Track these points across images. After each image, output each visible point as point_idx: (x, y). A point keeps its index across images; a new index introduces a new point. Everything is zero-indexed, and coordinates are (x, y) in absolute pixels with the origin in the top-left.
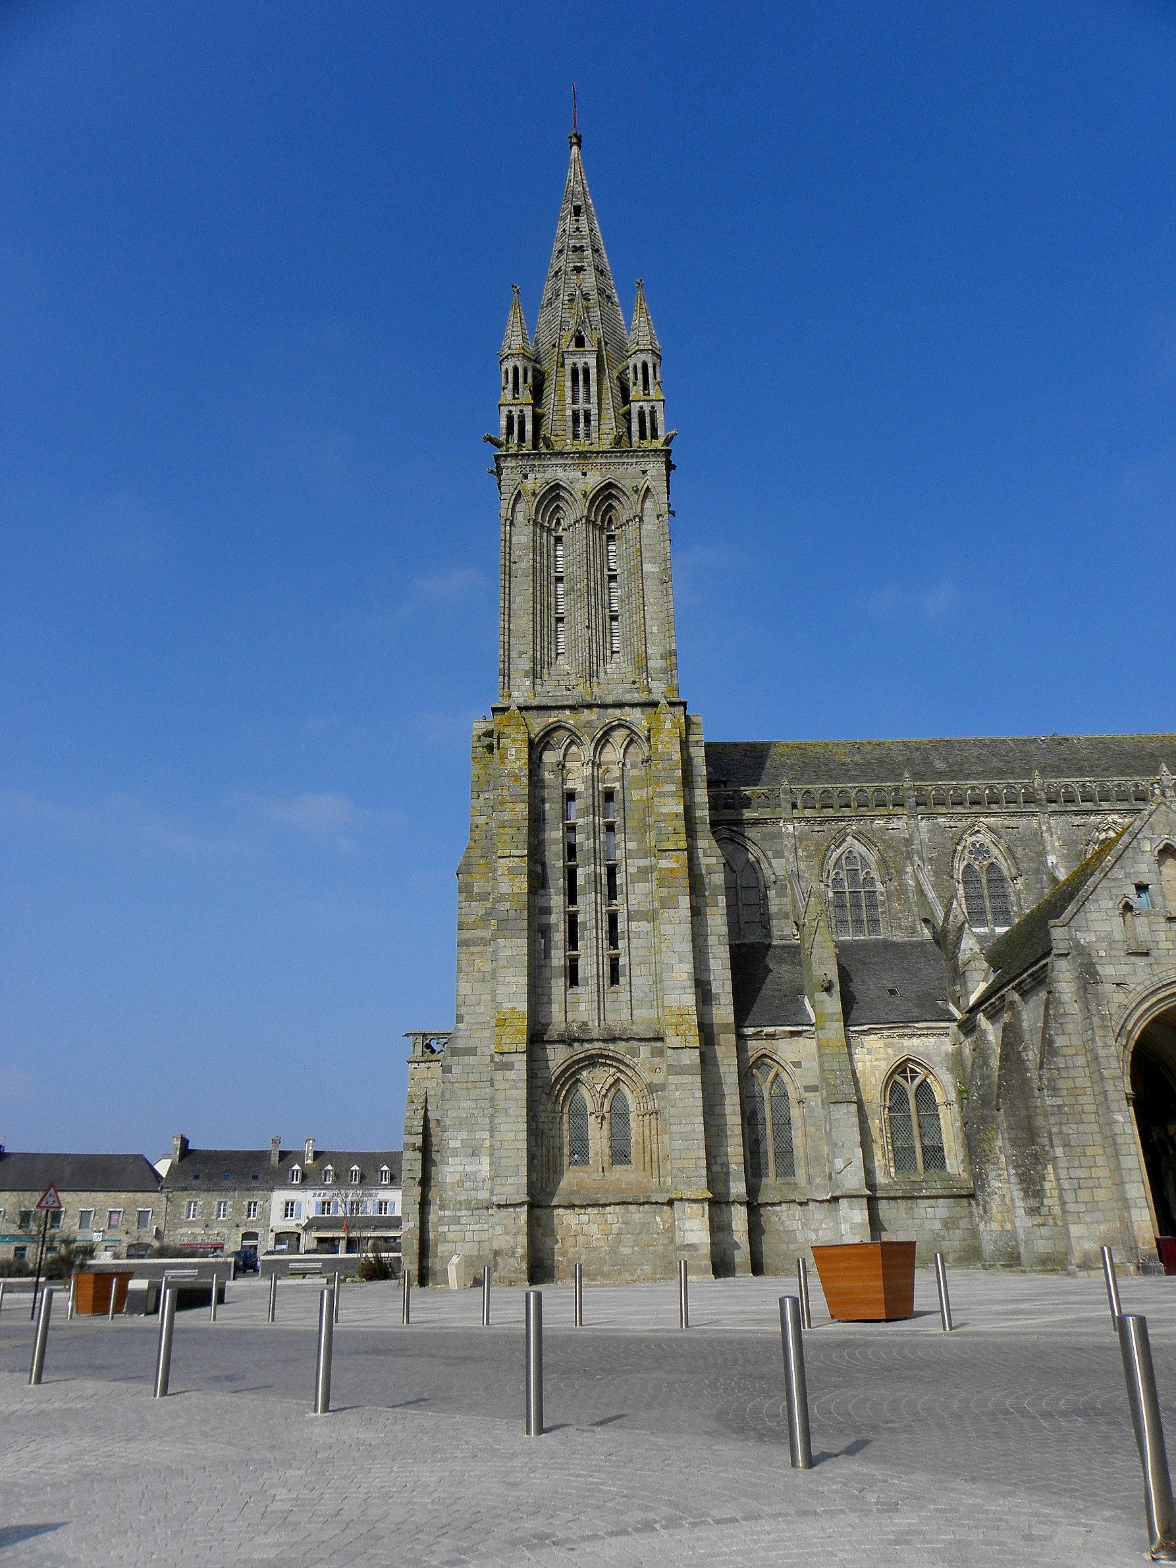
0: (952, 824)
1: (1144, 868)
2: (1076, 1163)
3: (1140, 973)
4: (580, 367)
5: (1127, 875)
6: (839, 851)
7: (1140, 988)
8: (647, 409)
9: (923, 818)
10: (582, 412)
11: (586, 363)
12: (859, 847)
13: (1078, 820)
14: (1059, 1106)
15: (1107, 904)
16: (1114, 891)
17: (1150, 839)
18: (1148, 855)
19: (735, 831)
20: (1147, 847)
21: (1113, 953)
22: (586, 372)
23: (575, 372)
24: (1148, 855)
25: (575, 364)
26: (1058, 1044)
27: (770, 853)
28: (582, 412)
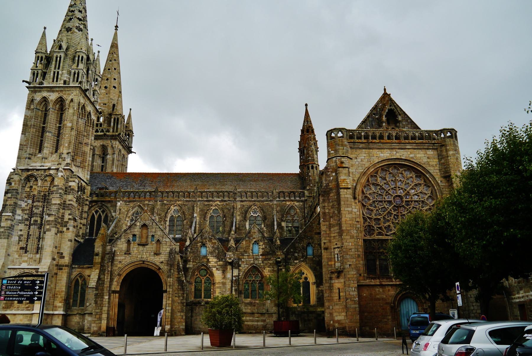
0: (168, 203)
1: (136, 230)
2: (98, 308)
3: (127, 259)
4: (59, 56)
5: (131, 232)
6: (134, 210)
7: (125, 263)
8: (77, 71)
9: (159, 201)
10: (56, 72)
11: (60, 56)
12: (139, 210)
13: (206, 203)
14: (97, 294)
15: (123, 240)
16: (126, 237)
17: (140, 222)
18: (138, 226)
19: (103, 204)
20: (138, 224)
21: (121, 253)
22: (60, 58)
23: (57, 58)
24: (138, 226)
25: (57, 56)
26: (101, 277)
27: (112, 211)
28: (56, 72)
